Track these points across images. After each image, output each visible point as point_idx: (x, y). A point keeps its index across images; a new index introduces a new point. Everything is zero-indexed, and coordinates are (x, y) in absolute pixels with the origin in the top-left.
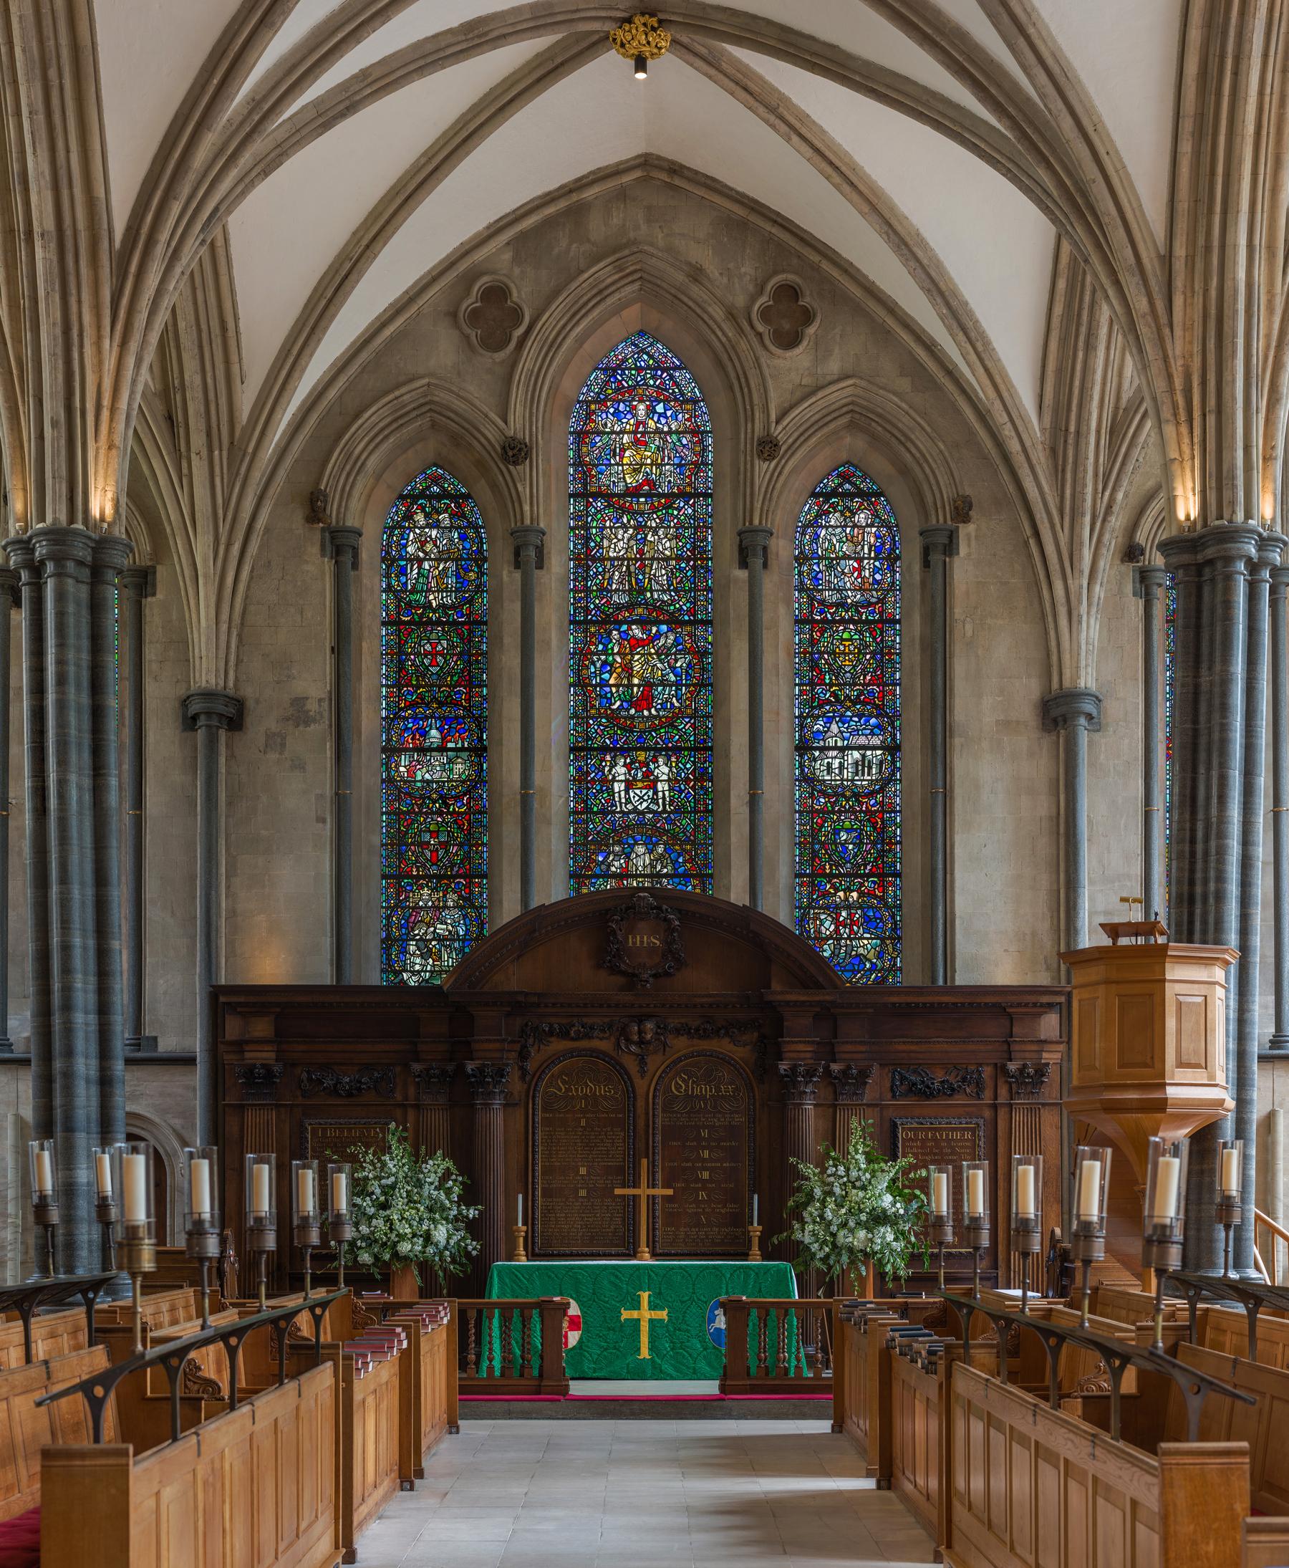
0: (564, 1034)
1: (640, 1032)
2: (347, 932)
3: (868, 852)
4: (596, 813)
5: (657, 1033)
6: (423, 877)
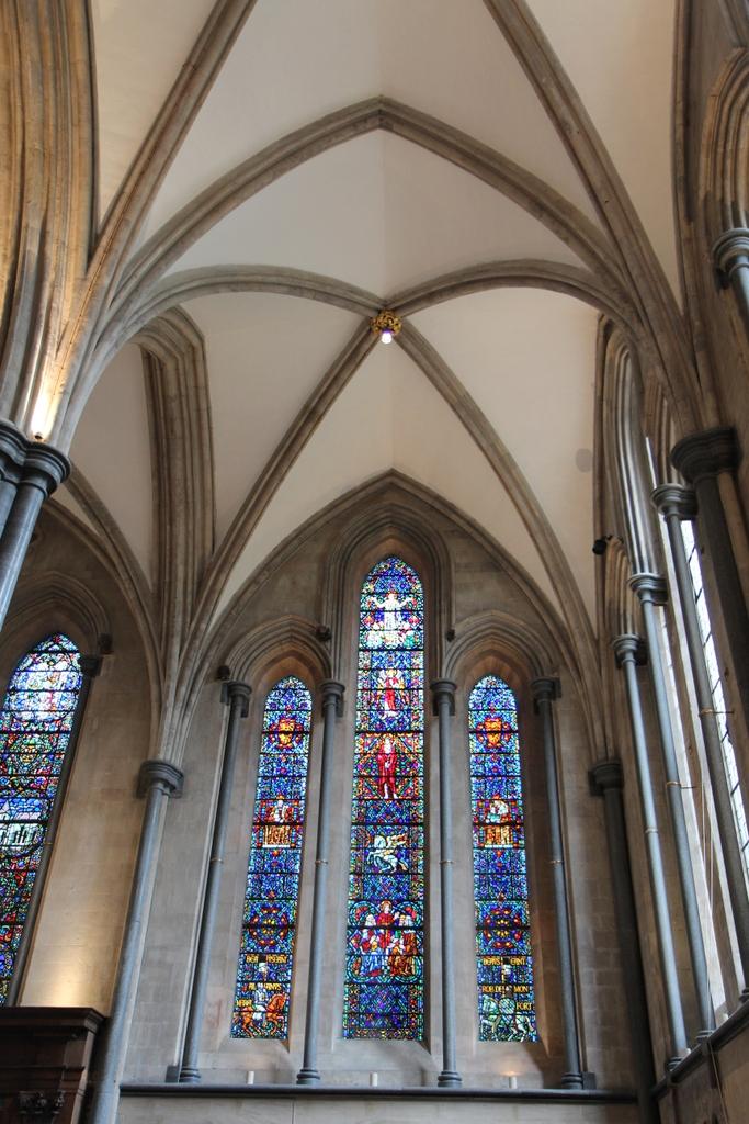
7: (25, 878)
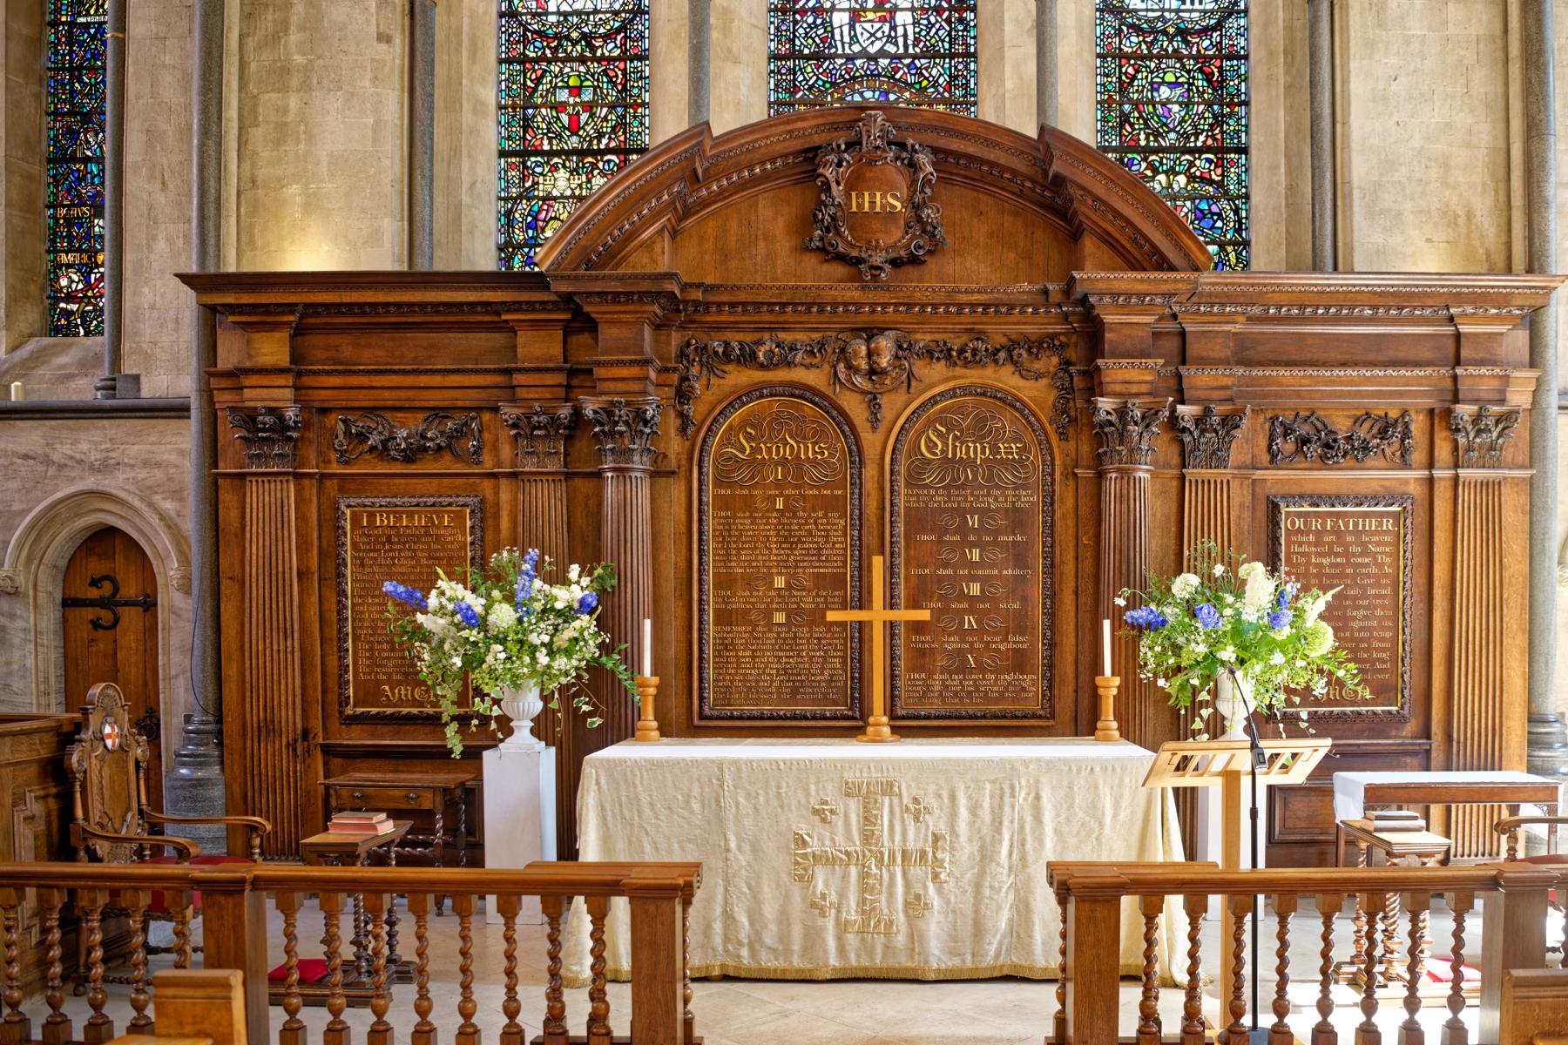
0: (747, 358)
1: (870, 355)
2: (422, 212)
3: (1201, 116)
4: (808, 58)
5: (897, 357)
6: (558, 153)
7: (1220, 69)
